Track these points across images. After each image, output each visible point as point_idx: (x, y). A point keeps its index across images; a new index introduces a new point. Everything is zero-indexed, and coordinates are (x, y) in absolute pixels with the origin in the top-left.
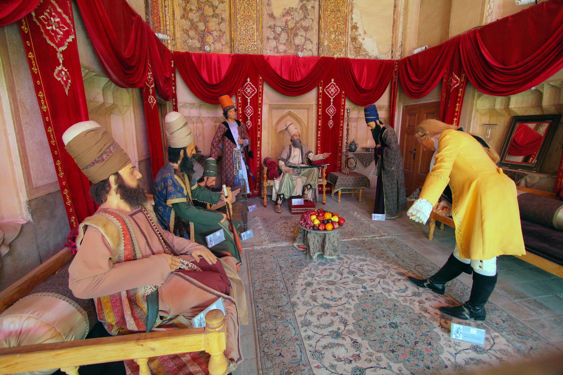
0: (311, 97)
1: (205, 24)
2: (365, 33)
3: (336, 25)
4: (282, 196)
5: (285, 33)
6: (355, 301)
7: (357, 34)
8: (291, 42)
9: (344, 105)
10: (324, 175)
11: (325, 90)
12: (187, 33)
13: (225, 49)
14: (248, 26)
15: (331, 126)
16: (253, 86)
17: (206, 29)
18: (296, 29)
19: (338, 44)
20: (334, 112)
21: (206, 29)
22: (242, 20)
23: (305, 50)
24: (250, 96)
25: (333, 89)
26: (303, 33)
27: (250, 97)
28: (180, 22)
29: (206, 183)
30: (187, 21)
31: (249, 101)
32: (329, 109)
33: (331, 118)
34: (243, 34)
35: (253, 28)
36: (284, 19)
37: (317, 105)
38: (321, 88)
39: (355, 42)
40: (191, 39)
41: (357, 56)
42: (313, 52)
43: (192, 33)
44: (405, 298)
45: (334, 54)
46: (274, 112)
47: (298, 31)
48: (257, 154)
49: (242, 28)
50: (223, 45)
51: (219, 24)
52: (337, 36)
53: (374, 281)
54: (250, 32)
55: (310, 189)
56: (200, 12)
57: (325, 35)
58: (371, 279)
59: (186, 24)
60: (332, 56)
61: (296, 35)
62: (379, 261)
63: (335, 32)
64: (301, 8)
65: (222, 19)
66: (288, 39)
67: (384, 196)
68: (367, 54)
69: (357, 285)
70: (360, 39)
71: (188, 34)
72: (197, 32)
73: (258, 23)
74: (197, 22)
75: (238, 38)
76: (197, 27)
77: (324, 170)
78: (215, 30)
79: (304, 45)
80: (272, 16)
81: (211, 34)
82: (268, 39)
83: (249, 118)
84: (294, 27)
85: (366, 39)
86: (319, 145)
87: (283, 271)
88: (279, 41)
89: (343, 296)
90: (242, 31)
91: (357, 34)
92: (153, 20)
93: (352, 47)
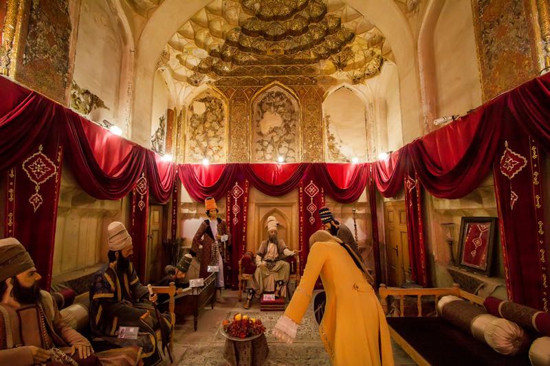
0: (293, 197)
2: (341, 141)
25: (312, 189)
26: (287, 145)
31: (236, 201)
36: (270, 136)
43: (197, 149)
45: (312, 160)
46: (261, 209)
56: (204, 135)
63: (313, 143)
64: (285, 126)
65: (221, 138)
66: (273, 151)
70: (337, 147)
80: (260, 134)
82: (257, 150)
85: (343, 147)
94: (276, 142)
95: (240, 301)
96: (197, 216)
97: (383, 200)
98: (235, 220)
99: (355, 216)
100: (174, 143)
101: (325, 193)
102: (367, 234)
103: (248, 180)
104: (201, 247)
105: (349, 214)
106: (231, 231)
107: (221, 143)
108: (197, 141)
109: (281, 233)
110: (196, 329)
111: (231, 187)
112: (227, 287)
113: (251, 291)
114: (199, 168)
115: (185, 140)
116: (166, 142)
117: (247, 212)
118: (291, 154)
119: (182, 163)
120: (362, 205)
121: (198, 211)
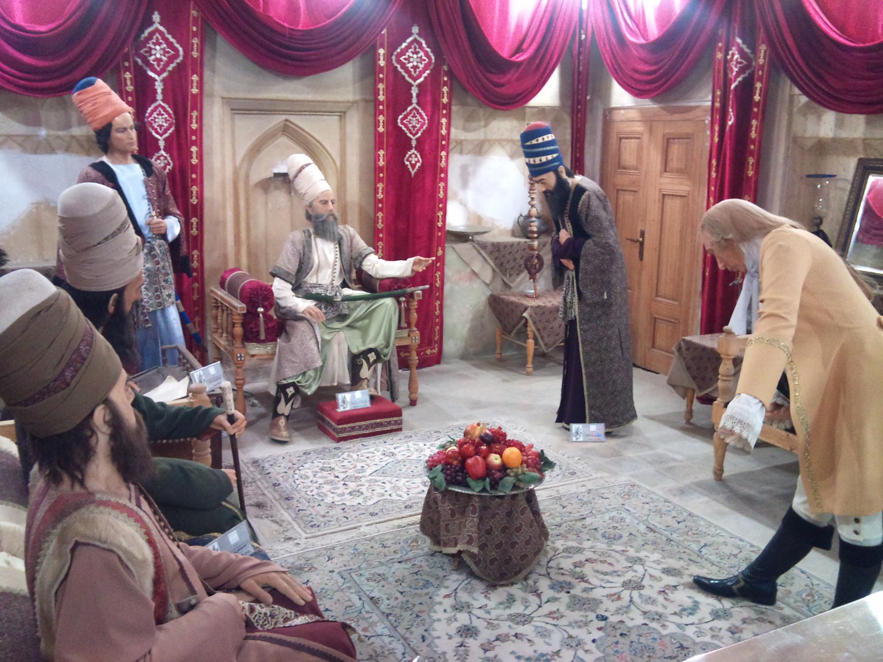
4: (290, 391)
6: (592, 653)
9: (448, 107)
10: (414, 316)
11: (394, 58)
15: (413, 166)
16: (172, 40)
20: (422, 127)
27: (165, 75)
31: (159, 87)
32: (405, 117)
33: (414, 143)
38: (381, 51)
44: (697, 627)
53: (619, 598)
55: (375, 362)
58: (611, 595)
62: (614, 547)
67: (583, 371)
69: (582, 613)
77: (415, 304)
83: (162, 144)
86: (380, 226)
87: (383, 607)
89: (562, 646)
103: (198, 6)
117: (199, 132)
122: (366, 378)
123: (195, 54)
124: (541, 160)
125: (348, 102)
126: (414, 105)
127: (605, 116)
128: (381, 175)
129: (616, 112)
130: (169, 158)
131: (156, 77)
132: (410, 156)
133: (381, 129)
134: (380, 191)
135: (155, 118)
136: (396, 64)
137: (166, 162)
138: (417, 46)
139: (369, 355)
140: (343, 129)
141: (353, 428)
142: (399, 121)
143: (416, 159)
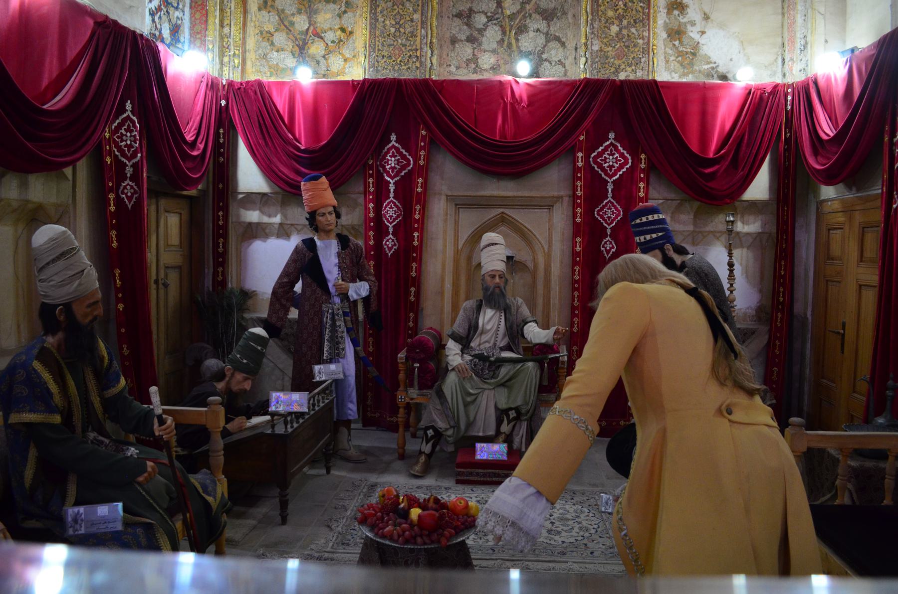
1: (310, 18)
2: (706, 17)
3: (621, 3)
5: (495, 27)
7: (683, 20)
8: (510, 45)
12: (268, 39)
13: (350, 69)
14: (402, 15)
15: (608, 252)
16: (405, 153)
17: (312, 28)
18: (524, 17)
19: (627, 47)
20: (617, 217)
21: (312, 28)
22: (390, 4)
23: (546, 64)
24: (395, 176)
26: (543, 25)
28: (256, 16)
29: (228, 383)
30: (271, 14)
31: (392, 188)
32: (602, 209)
33: (609, 232)
34: (389, 35)
35: (412, 20)
37: (572, 199)
38: (580, 155)
39: (681, 42)
40: (278, 51)
41: (685, 75)
42: (567, 67)
43: (280, 38)
45: (617, 71)
47: (528, 21)
48: (407, 319)
49: (388, 22)
50: (345, 60)
51: (340, 16)
52: (625, 28)
54: (405, 28)
57: (593, 28)
59: (269, 20)
60: (613, 77)
61: (522, 30)
63: (620, 18)
66: (502, 40)
68: (713, 68)
70: (693, 33)
71: (272, 42)
72: (291, 36)
73: (426, 9)
74: (293, 15)
75: (377, 43)
76: (292, 24)
78: (331, 29)
79: (543, 53)
81: (322, 38)
82: (454, 41)
83: (391, 230)
84: (518, 12)
85: (710, 33)
86: (576, 303)
88: (480, 44)
90: (387, 28)
91: (685, 20)
92: (193, 18)
93: (670, 52)
94: (512, 17)
95: (402, 457)
96: (283, 232)
97: (816, 192)
98: (390, 243)
99: (732, 241)
100: (214, 20)
101: (647, 171)
102: (761, 291)
104: (294, 314)
105: (716, 235)
106: (378, 275)
107: (348, 20)
108: (280, 13)
109: (518, 282)
110: (284, 521)
111: (379, 153)
112: (368, 422)
113: (430, 433)
114: (286, 91)
115: (245, 12)
116: (192, 15)
117: (422, 221)
118: (555, 52)
119: (237, 78)
120: (755, 207)
121: (285, 216)
122: (504, 433)
123: (422, 163)
124: (645, 239)
125: (553, 197)
126: (610, 199)
127: (818, 209)
128: (578, 259)
129: (825, 204)
130: (395, 241)
131: (391, 181)
132: (606, 243)
133: (578, 220)
134: (577, 272)
135: (388, 210)
136: (593, 165)
137: (393, 243)
138: (613, 149)
139: (510, 413)
140: (550, 219)
141: (471, 474)
142: (596, 213)
143: (611, 246)
